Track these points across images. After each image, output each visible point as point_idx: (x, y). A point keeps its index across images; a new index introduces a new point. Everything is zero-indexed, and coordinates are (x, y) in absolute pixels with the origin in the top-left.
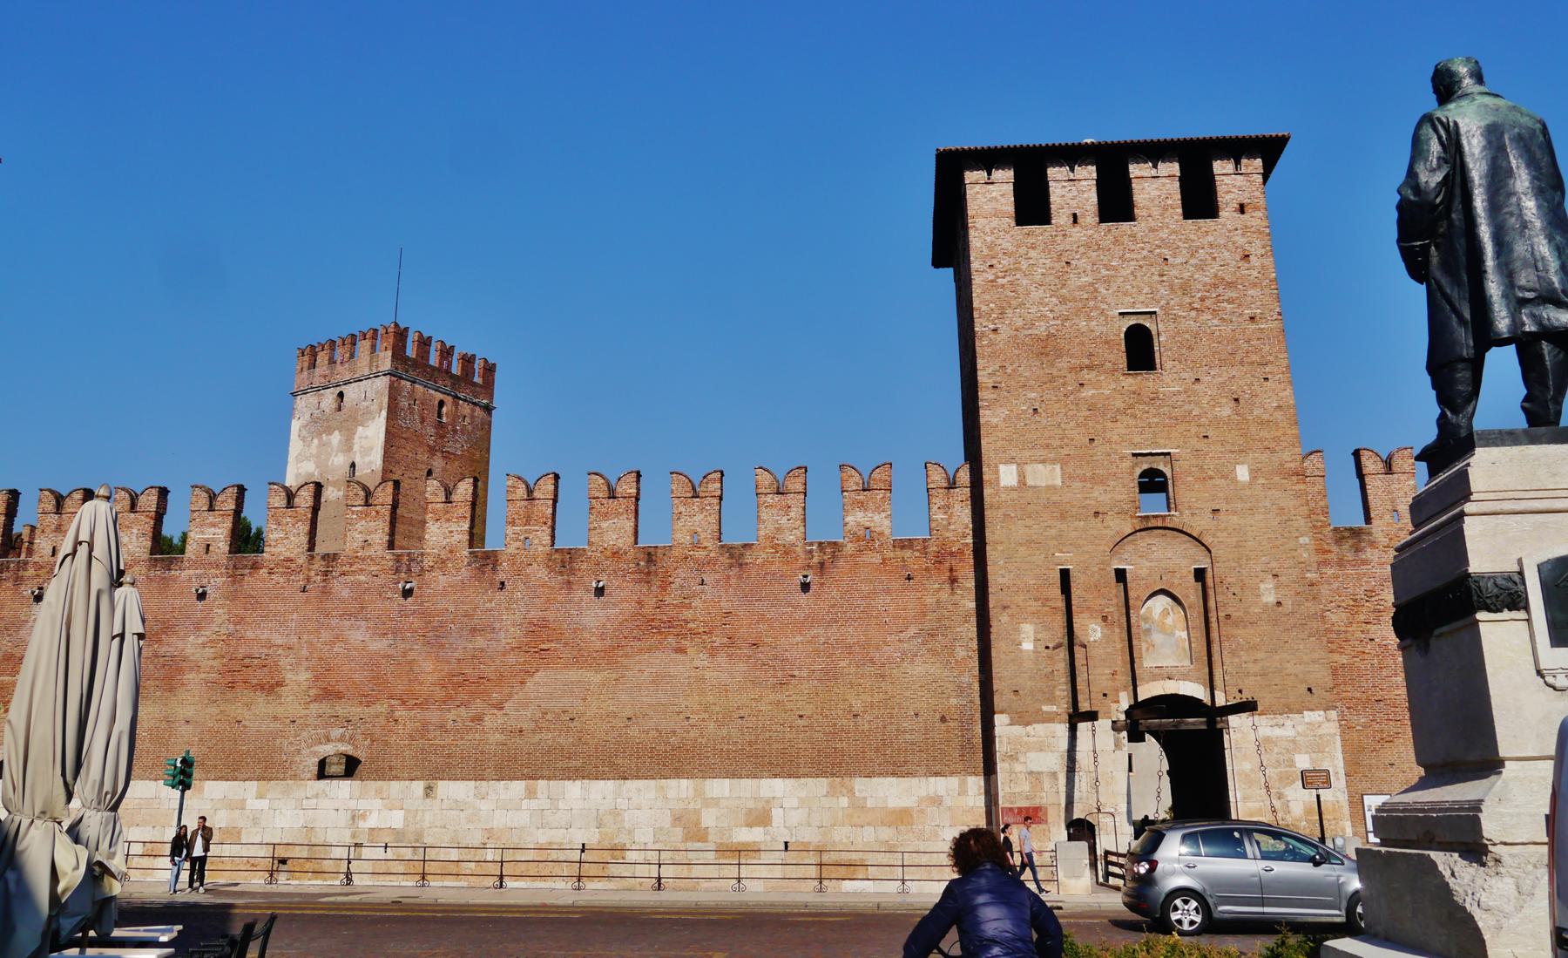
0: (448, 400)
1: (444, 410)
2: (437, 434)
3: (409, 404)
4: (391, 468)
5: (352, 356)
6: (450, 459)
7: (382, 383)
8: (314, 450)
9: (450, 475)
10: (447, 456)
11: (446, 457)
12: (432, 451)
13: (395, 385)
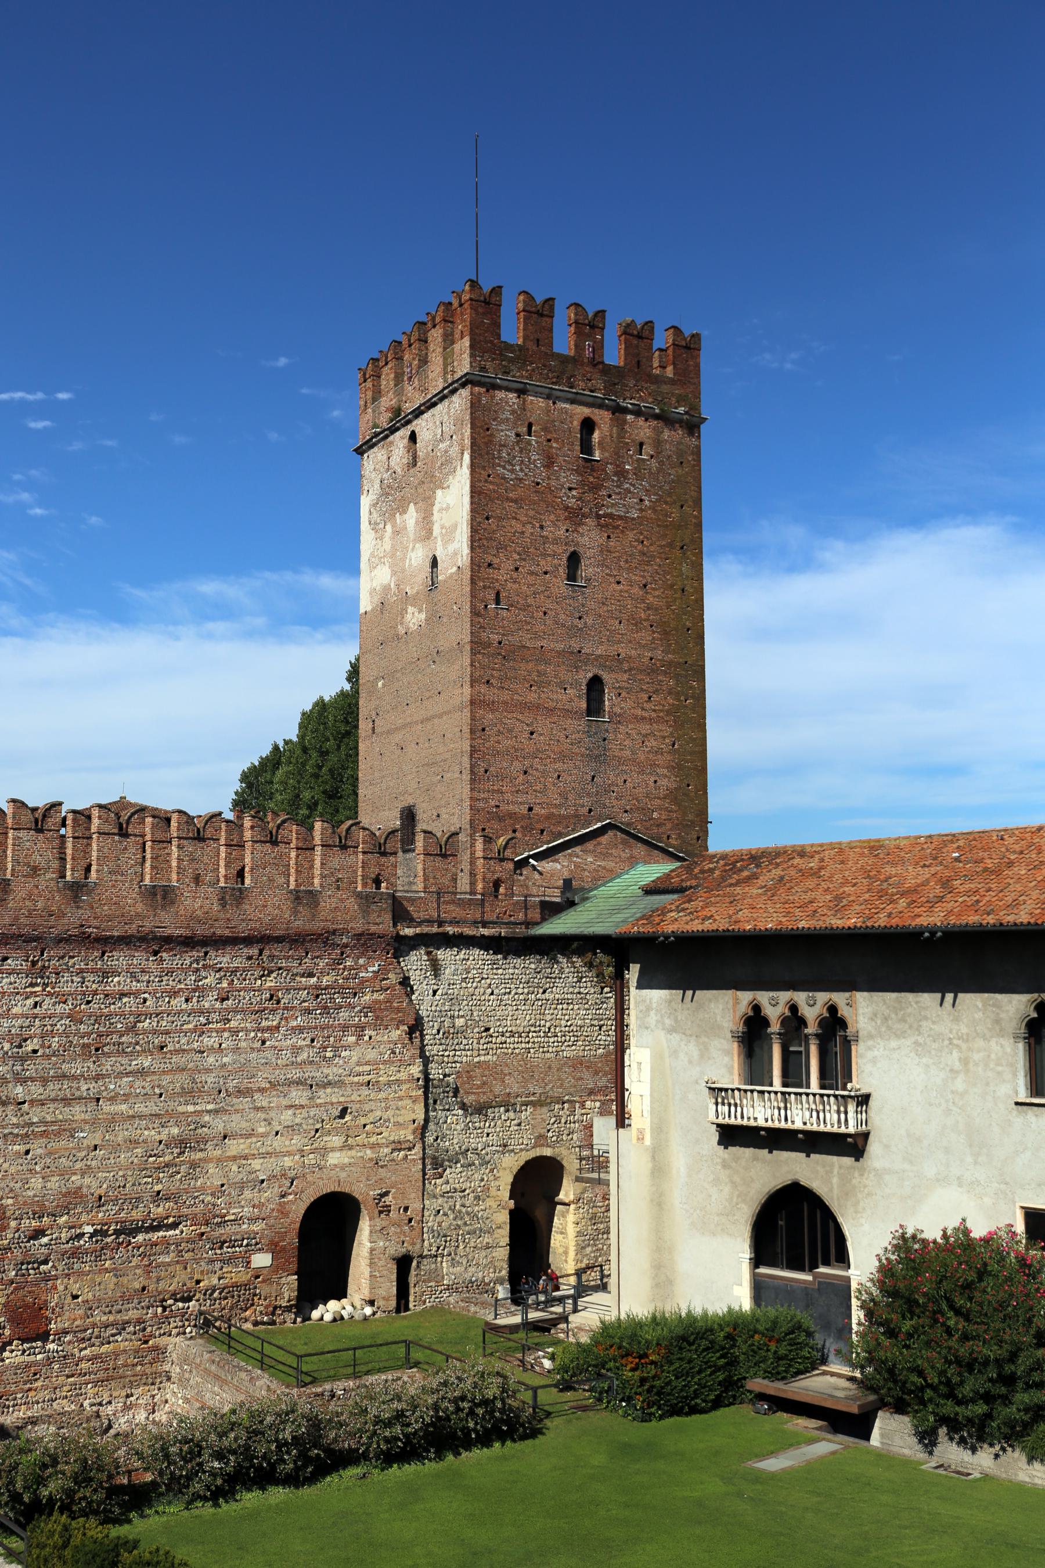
0: (602, 417)
1: (596, 436)
2: (582, 483)
3: (518, 435)
4: (489, 558)
5: (424, 361)
6: (617, 527)
7: (460, 401)
8: (387, 544)
9: (619, 558)
10: (609, 524)
11: (607, 526)
12: (575, 517)
13: (484, 400)
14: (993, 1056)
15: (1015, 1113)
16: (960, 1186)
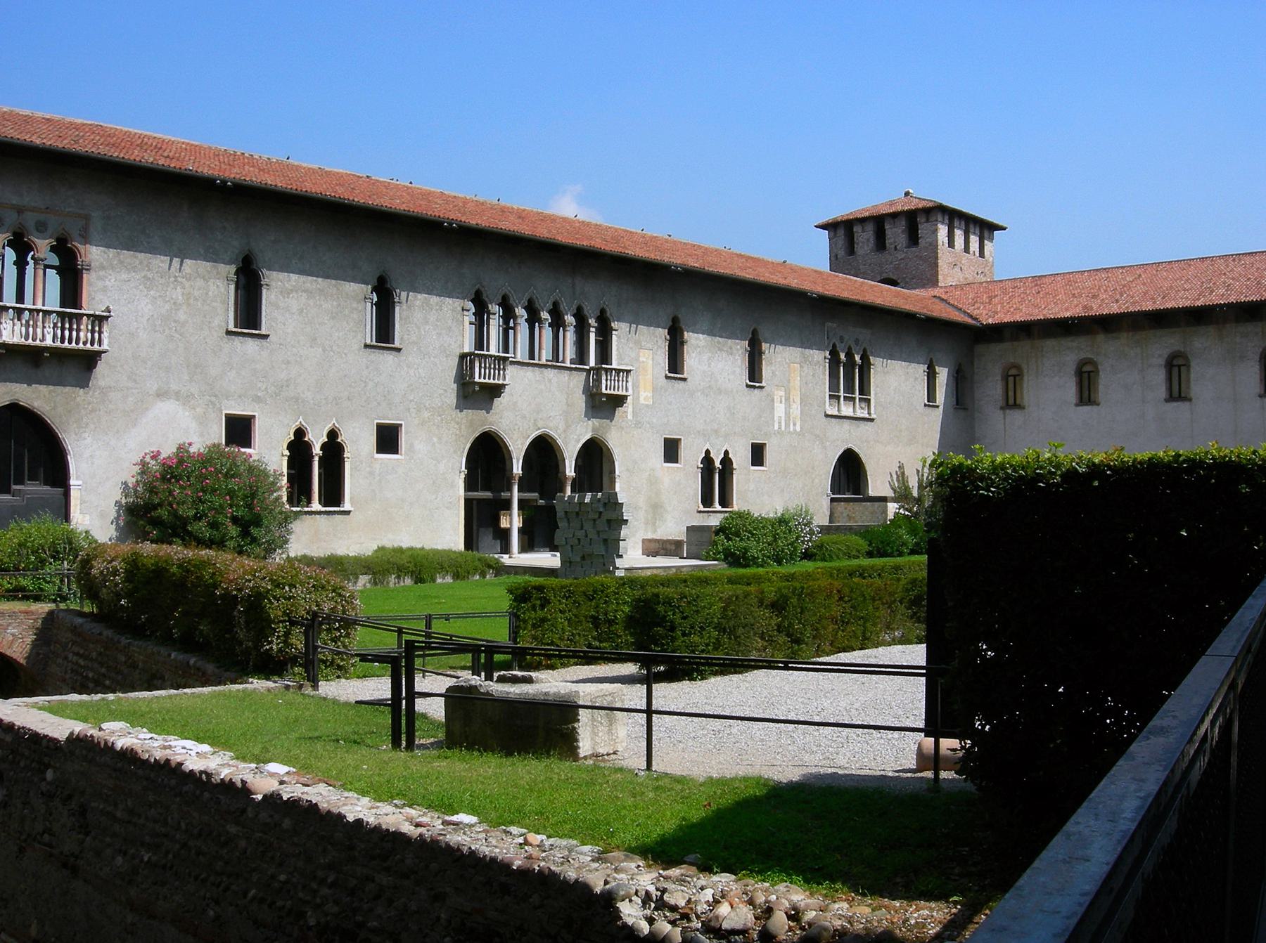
14: (210, 293)
15: (225, 340)
16: (178, 400)
